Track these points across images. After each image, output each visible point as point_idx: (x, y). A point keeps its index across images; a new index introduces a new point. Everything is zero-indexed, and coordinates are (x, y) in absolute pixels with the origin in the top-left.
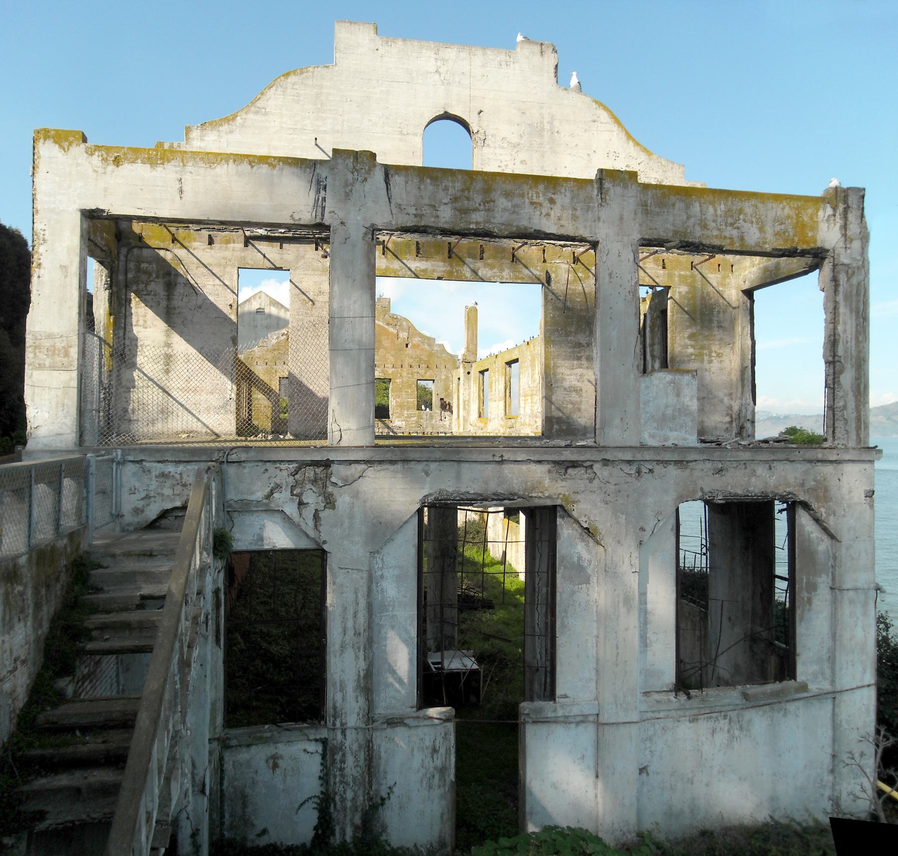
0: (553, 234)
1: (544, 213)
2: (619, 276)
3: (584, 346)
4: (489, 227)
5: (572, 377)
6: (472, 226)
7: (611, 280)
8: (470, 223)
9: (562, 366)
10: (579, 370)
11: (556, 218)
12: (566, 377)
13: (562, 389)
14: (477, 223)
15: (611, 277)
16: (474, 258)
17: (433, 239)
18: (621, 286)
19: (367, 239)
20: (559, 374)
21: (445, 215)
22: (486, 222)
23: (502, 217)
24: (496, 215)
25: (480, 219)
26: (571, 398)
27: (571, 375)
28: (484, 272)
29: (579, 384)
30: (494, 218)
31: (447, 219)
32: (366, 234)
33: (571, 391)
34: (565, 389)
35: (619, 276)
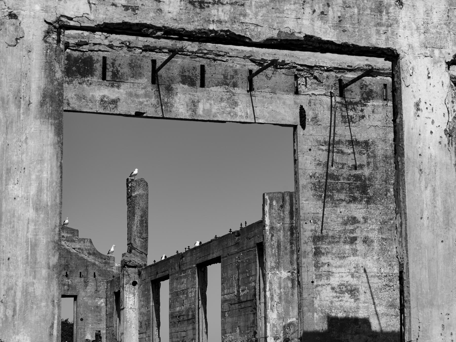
0: (331, 43)
1: (318, 12)
2: (430, 108)
3: (359, 222)
4: (237, 29)
5: (342, 270)
6: (212, 27)
7: (419, 112)
8: (208, 22)
9: (327, 253)
10: (352, 258)
11: (337, 19)
12: (334, 270)
13: (329, 288)
14: (220, 22)
15: (418, 109)
16: (192, 84)
17: (128, 55)
18: (433, 122)
19: (50, 40)
20: (323, 264)
21: (171, 9)
22: (233, 20)
23: (256, 14)
24: (248, 11)
25: (223, 17)
26: (342, 303)
27: (340, 267)
28: (207, 106)
29: (353, 281)
30: (245, 15)
31: (174, 14)
32: (48, 33)
33: (342, 292)
34: (333, 289)
35: (430, 108)
